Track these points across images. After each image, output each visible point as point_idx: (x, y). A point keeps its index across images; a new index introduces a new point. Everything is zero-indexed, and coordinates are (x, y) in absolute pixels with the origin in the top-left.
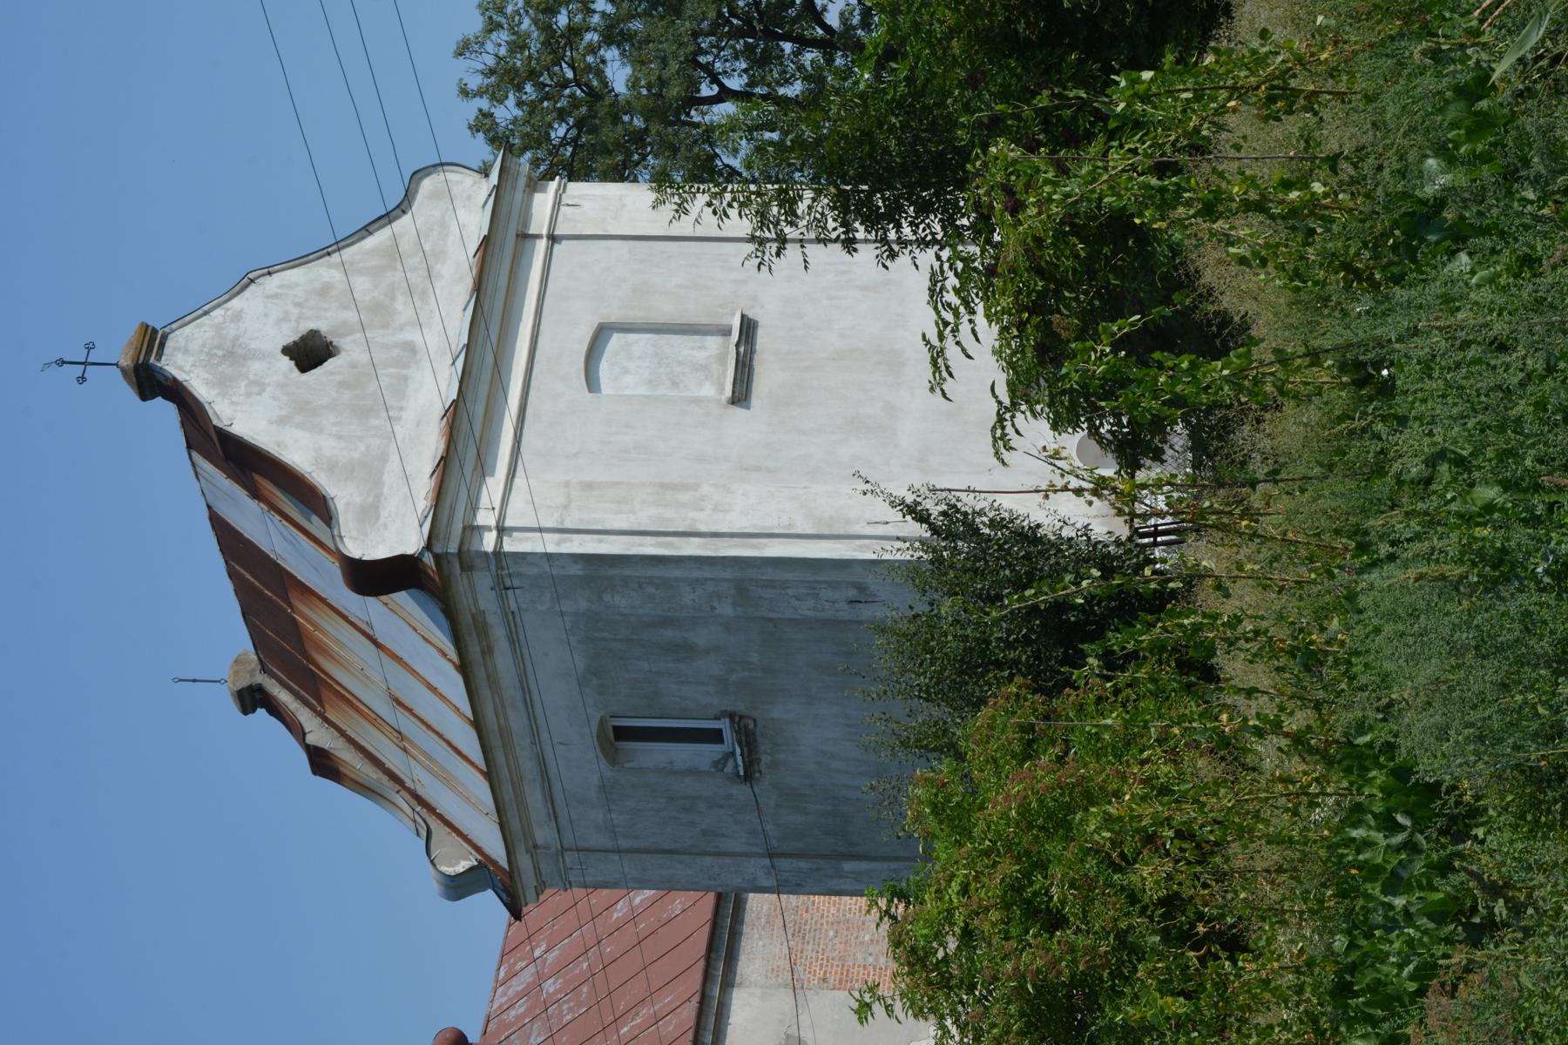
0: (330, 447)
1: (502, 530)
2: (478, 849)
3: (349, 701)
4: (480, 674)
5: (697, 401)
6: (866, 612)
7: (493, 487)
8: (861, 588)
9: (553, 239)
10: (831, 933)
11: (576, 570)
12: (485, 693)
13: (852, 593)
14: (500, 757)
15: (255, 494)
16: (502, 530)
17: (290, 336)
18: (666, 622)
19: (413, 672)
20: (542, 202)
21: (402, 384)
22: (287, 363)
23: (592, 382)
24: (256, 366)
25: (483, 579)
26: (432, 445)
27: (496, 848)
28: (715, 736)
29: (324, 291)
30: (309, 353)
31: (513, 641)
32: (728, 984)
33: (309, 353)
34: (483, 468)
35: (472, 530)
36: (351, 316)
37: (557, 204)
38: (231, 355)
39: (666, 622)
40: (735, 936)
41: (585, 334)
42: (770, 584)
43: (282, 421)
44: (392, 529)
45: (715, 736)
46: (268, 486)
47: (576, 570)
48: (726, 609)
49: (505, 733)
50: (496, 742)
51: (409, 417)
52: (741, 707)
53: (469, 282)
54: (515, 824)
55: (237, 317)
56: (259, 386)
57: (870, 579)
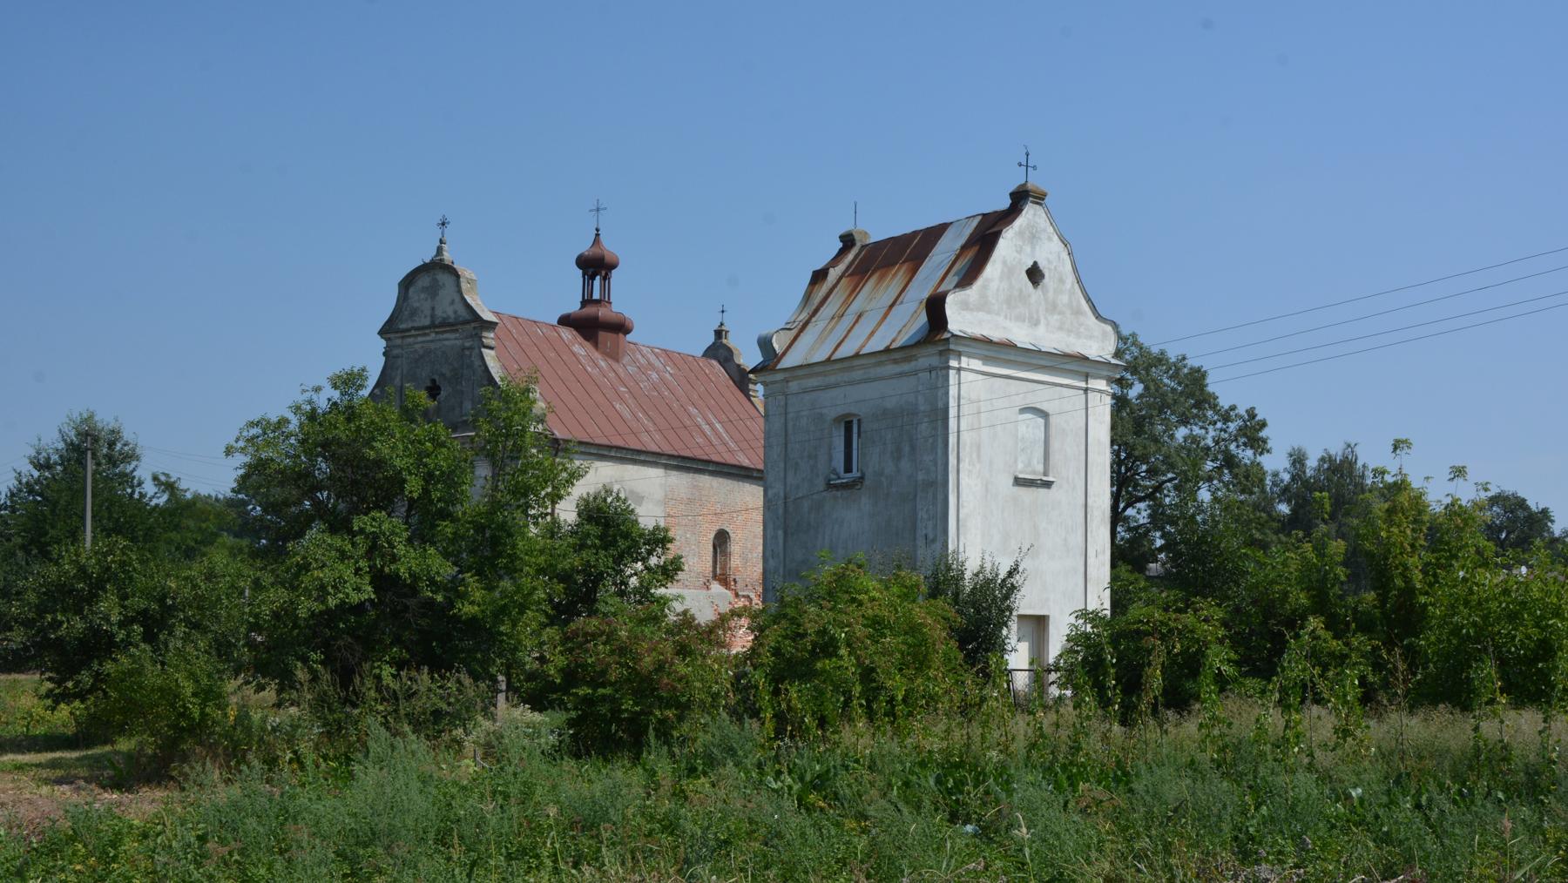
0: (994, 285)
1: (959, 370)
2: (784, 354)
3: (855, 290)
4: (884, 358)
5: (1016, 461)
6: (920, 542)
7: (976, 364)
8: (933, 541)
9: (1086, 390)
11: (940, 405)
12: (873, 360)
13: (931, 536)
14: (838, 366)
15: (964, 248)
16: (959, 370)
17: (1042, 265)
18: (913, 448)
19: (879, 324)
20: (1101, 384)
21: (1020, 318)
22: (1030, 264)
23: (1024, 410)
24: (1028, 249)
25: (935, 361)
26: (996, 335)
27: (786, 363)
28: (848, 469)
29: (1062, 281)
30: (1035, 274)
31: (901, 375)
32: (666, 467)
33: (1035, 274)
34: (986, 360)
35: (959, 355)
36: (1051, 294)
37: (1100, 391)
38: (1033, 237)
39: (913, 448)
40: (688, 470)
41: (1044, 407)
42: (935, 497)
43: (1004, 263)
44: (959, 319)
45: (848, 469)
46: (970, 254)
47: (940, 405)
48: (921, 476)
49: (851, 368)
50: (846, 364)
51: (1008, 324)
52: (867, 482)
53: (1068, 351)
54: (800, 373)
55: (1050, 239)
56: (1020, 251)
57: (938, 545)
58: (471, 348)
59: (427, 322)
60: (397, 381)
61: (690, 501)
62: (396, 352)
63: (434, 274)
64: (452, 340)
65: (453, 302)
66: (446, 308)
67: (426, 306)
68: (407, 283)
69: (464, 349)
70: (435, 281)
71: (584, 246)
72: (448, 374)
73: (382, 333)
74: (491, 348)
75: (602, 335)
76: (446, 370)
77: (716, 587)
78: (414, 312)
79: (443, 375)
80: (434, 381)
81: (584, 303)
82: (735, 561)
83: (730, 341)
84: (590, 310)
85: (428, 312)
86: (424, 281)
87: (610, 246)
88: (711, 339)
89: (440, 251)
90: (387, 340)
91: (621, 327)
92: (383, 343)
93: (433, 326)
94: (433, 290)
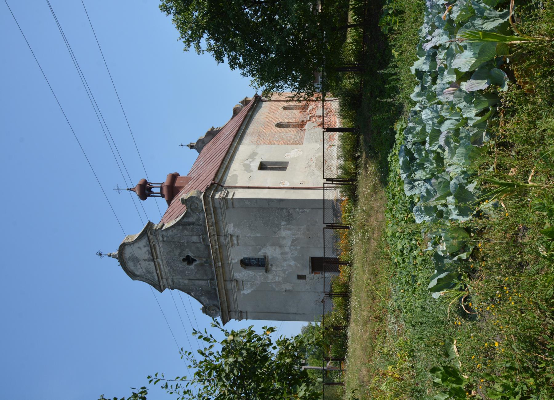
58: (163, 236)
59: (152, 263)
60: (186, 282)
61: (259, 136)
62: (170, 283)
63: (122, 255)
64: (160, 249)
65: (139, 248)
66: (141, 251)
67: (144, 264)
68: (133, 275)
69: (163, 241)
70: (129, 258)
71: (135, 195)
72: (179, 251)
73: (161, 291)
74: (163, 225)
75: (177, 184)
76: (177, 252)
77: (306, 127)
78: (149, 272)
79: (180, 254)
80: (184, 260)
81: (163, 196)
83: (194, 142)
84: (165, 192)
85: (147, 263)
86: (131, 265)
87: (136, 182)
88: (194, 151)
89: (114, 257)
90: (165, 288)
91: (174, 177)
92: (167, 290)
93: (153, 260)
94: (136, 260)
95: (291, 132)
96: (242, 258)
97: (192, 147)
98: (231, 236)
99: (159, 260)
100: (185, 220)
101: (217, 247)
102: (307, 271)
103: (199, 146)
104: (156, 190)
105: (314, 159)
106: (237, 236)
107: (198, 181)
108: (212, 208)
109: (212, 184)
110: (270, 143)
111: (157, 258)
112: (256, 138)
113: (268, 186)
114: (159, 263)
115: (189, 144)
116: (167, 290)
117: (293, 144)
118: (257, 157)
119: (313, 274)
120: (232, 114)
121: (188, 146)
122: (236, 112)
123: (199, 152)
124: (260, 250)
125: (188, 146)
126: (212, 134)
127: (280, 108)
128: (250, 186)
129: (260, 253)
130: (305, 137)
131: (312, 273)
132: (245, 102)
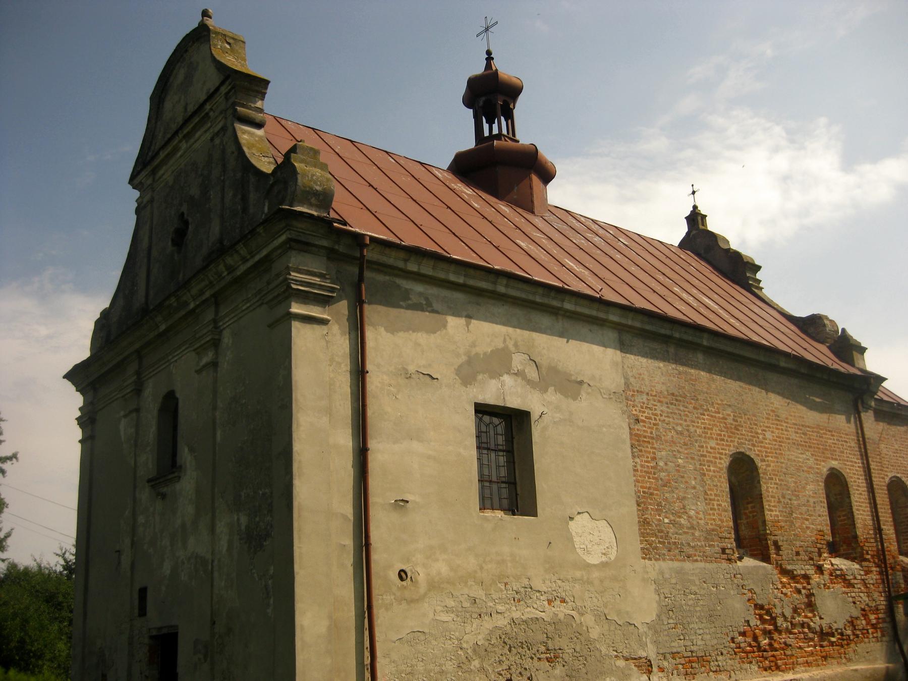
10: (679, 429)
82: (772, 512)
83: (713, 225)
88: (682, 230)
95: (713, 509)
96: (178, 395)
97: (695, 219)
98: (216, 344)
99: (184, 145)
100: (252, 179)
101: (192, 306)
102: (155, 620)
103: (700, 238)
104: (500, 126)
105: (562, 611)
106: (214, 364)
107: (633, 269)
108: (264, 252)
109: (358, 238)
110: (638, 442)
111: (187, 137)
112: (659, 387)
113: (372, 444)
114: (176, 149)
115: (703, 210)
116: (136, 194)
117: (644, 523)
118: (552, 396)
119: (146, 641)
120: (801, 311)
121: (695, 207)
122: (813, 326)
123: (684, 244)
124: (192, 450)
125: (695, 207)
126: (737, 270)
127: (834, 464)
128: (374, 382)
129: (186, 450)
130: (688, 565)
131: (151, 637)
132: (846, 347)
